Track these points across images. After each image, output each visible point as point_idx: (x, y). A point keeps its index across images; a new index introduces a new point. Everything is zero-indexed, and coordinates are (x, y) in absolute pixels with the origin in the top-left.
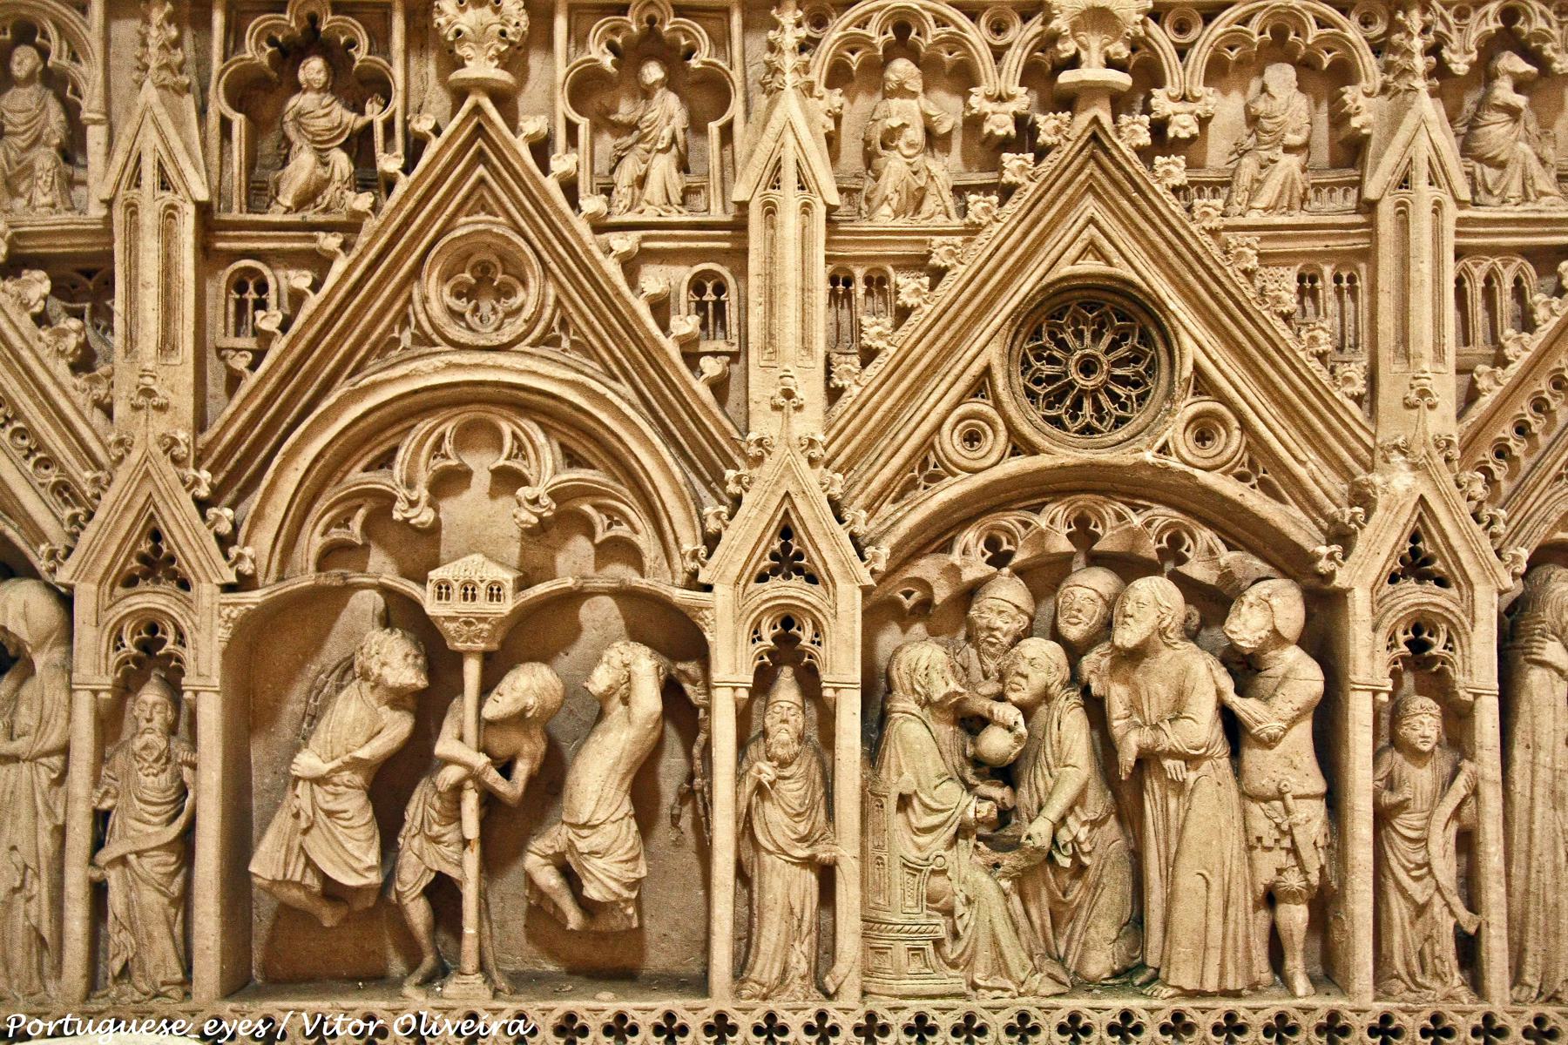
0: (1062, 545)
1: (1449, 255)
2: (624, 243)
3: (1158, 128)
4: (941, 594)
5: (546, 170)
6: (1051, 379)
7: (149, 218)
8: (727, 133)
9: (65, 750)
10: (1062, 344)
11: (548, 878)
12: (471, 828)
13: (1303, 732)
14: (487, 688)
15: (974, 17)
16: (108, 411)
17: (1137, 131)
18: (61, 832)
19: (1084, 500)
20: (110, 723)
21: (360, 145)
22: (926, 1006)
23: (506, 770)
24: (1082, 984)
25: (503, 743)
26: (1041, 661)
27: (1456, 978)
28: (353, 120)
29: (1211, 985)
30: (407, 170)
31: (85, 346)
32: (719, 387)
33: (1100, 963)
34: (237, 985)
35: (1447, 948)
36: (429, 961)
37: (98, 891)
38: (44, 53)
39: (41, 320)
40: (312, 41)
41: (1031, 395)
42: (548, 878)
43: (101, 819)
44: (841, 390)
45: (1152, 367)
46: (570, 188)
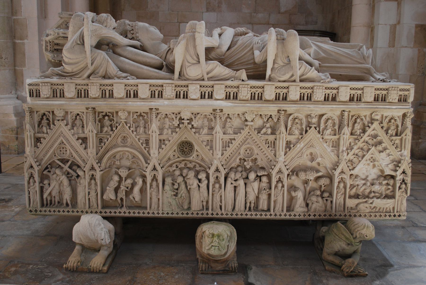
0: (184, 166)
1: (221, 140)
2: (138, 137)
3: (193, 125)
4: (171, 171)
5: (130, 130)
6: (182, 149)
7: (91, 136)
8: (148, 125)
9: (85, 186)
10: (183, 146)
11: (132, 198)
12: (124, 194)
13: (206, 186)
14: (125, 180)
15: (173, 113)
16: (88, 153)
17: (190, 126)
18: (85, 194)
19: (186, 162)
20: (90, 184)
21: (111, 126)
22: (168, 211)
23: (127, 188)
24: (184, 209)
25: (127, 186)
26: (180, 179)
27: (219, 210)
28: (111, 123)
29: (196, 210)
30: (116, 129)
31: (86, 146)
32: (148, 151)
33: (186, 207)
34: (103, 207)
35: (219, 207)
36: (121, 205)
37: (89, 199)
38: (80, 116)
39: (81, 144)
40: (106, 115)
41: (180, 151)
42: (132, 198)
43: (89, 192)
44: (159, 152)
45: (192, 149)
46: (133, 131)
